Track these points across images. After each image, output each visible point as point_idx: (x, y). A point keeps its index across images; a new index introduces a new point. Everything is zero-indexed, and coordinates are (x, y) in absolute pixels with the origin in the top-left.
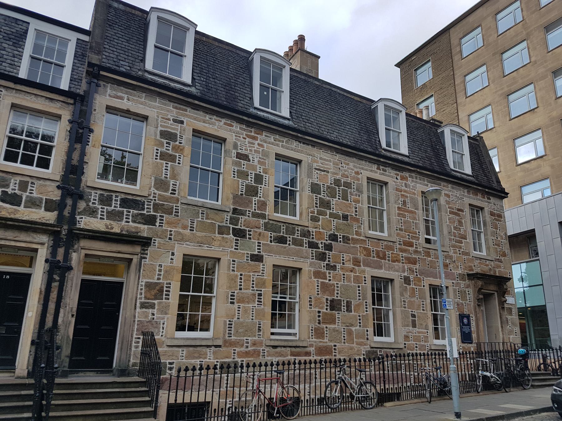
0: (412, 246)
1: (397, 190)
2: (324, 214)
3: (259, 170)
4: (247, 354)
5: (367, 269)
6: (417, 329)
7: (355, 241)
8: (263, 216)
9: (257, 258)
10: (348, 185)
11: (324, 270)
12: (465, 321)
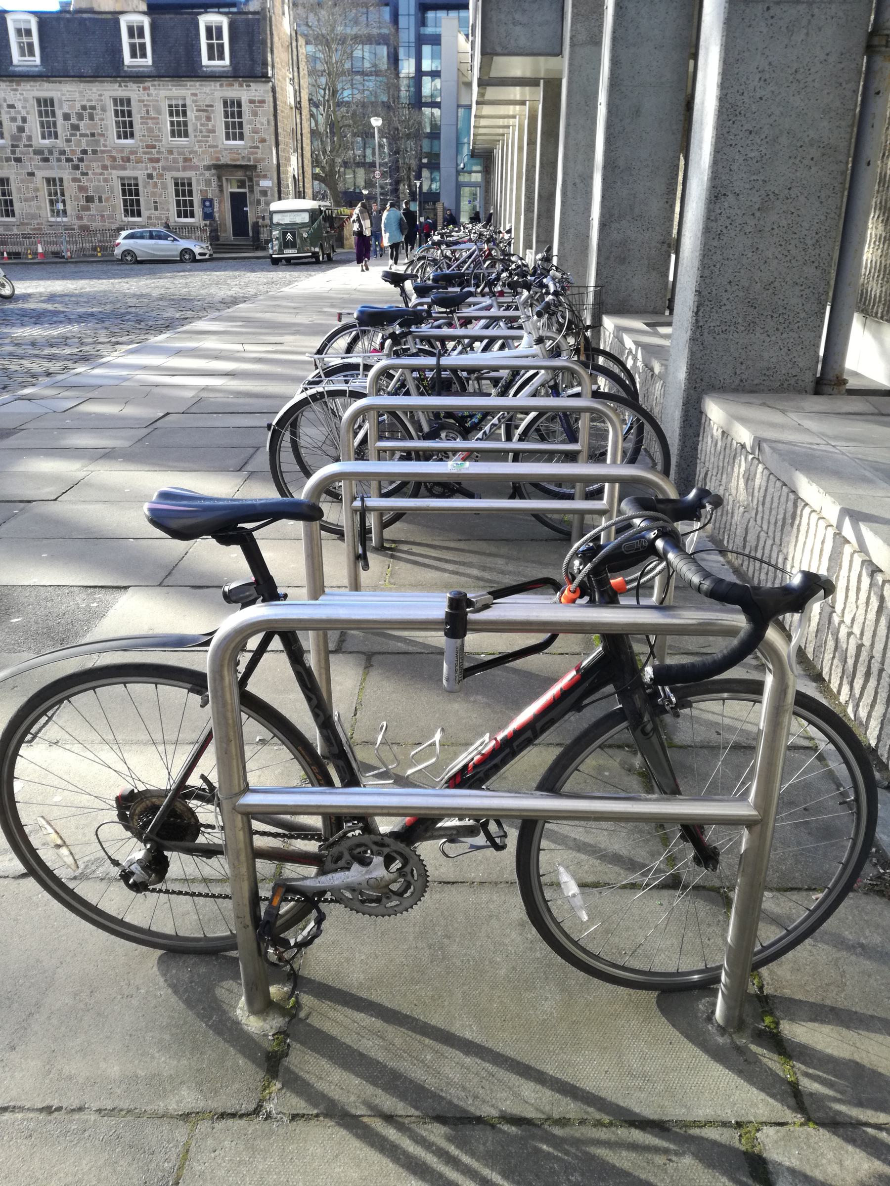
1: (139, 101)
2: (75, 135)
3: (24, 113)
4: (35, 229)
5: (114, 172)
7: (103, 152)
8: (31, 146)
9: (31, 174)
10: (93, 108)
11: (79, 176)
12: (207, 204)
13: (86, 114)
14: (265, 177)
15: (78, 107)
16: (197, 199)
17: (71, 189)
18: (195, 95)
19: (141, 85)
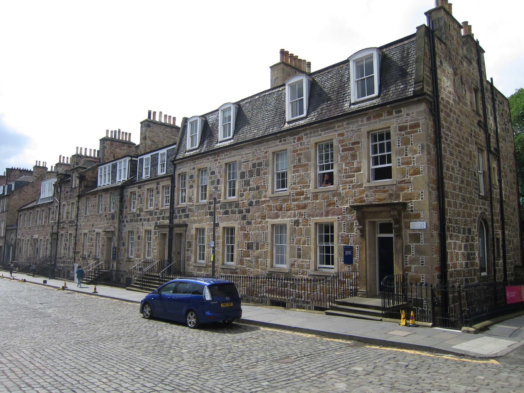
0: (303, 194)
1: (294, 151)
5: (269, 220)
6: (301, 260)
10: (260, 164)
13: (255, 170)
14: (417, 217)
15: (250, 164)
16: (337, 246)
17: (238, 236)
18: (342, 135)
19: (296, 137)
